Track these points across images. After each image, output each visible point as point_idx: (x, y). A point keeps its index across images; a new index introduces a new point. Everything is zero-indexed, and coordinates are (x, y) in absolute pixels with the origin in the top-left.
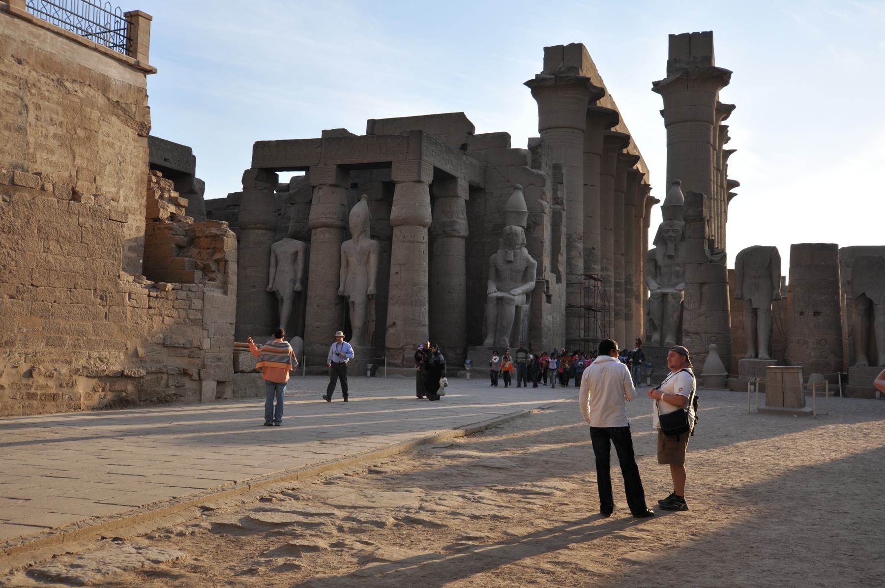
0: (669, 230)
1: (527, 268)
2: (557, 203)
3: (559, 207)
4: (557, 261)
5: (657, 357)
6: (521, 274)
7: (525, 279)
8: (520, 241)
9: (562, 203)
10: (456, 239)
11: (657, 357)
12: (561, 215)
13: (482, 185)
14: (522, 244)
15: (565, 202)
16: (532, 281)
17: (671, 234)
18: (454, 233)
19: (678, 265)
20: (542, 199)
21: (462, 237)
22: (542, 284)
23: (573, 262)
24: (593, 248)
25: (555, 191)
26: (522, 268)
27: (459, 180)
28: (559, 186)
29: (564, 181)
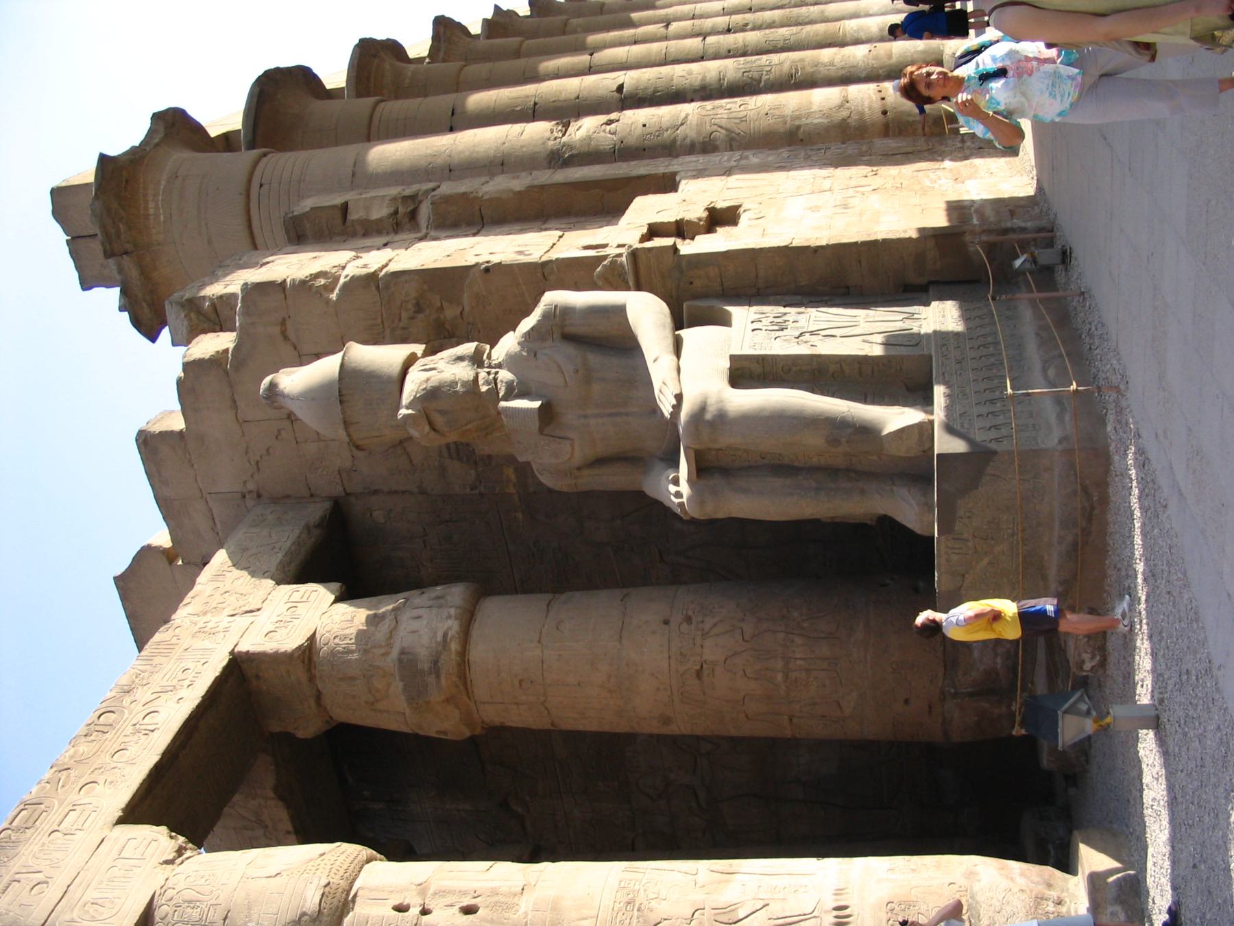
2: (413, 215)
3: (425, 211)
7: (618, 342)
8: (464, 372)
10: (479, 652)
12: (447, 199)
13: (316, 511)
14: (477, 360)
15: (409, 191)
16: (620, 310)
18: (449, 661)
20: (329, 288)
21: (468, 618)
22: (638, 271)
26: (565, 355)
27: (248, 645)
28: (353, 216)
29: (338, 200)
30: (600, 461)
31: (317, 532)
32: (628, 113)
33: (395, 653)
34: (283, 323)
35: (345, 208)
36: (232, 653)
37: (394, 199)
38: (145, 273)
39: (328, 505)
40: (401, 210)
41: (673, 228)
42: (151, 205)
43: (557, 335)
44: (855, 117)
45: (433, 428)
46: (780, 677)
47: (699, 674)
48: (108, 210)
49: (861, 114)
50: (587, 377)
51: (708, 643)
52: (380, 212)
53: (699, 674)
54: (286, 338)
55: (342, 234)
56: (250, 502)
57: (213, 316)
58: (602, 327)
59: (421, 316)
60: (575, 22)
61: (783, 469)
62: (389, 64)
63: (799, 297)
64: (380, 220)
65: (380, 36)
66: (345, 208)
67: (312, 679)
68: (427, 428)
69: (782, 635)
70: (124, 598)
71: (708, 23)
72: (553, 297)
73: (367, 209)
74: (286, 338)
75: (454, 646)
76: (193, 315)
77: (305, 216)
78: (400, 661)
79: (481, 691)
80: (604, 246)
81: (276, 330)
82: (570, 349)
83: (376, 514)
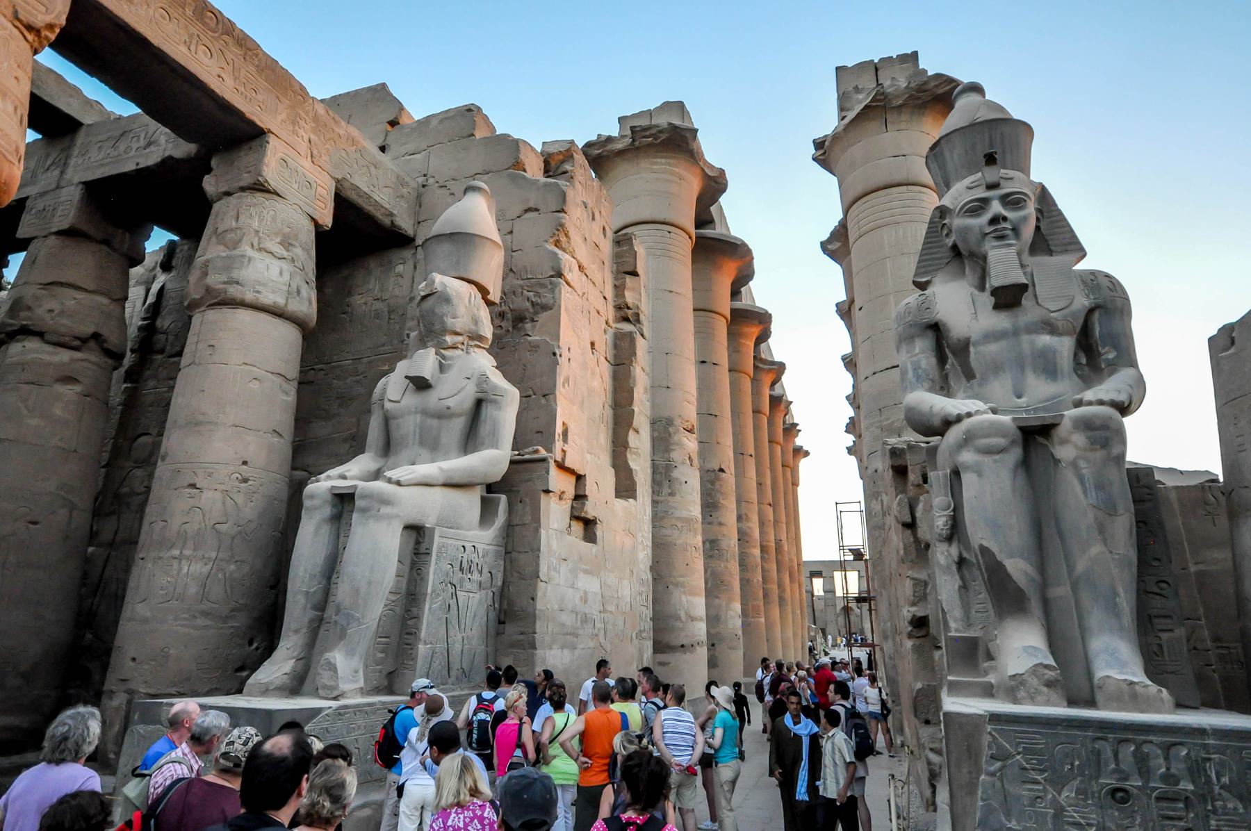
0: (985, 202)
1: (479, 403)
3: (627, 327)
4: (626, 446)
5: (1119, 796)
6: (458, 426)
9: (638, 321)
10: (243, 315)
11: (1119, 796)
16: (495, 445)
17: (996, 207)
18: (233, 291)
19: (1050, 328)
20: (557, 243)
23: (675, 474)
24: (722, 470)
25: (619, 289)
28: (629, 279)
29: (640, 270)
30: (387, 420)
31: (387, 221)
32: (698, 474)
33: (250, 252)
34: (536, 210)
35: (634, 274)
36: (270, 131)
37: (638, 308)
38: (621, 153)
39: (410, 232)
40: (630, 312)
41: (581, 493)
42: (663, 161)
43: (480, 395)
44: (678, 624)
45: (424, 298)
46: (176, 552)
47: (193, 486)
48: (661, 132)
49: (682, 629)
50: (444, 415)
51: (218, 495)
52: (630, 297)
53: (193, 486)
54: (526, 211)
55: (618, 272)
56: (421, 180)
57: (560, 170)
58: (484, 429)
59: (528, 305)
60: (779, 449)
61: (332, 566)
62: (754, 331)
63: (500, 583)
64: (624, 296)
65: (773, 327)
66: (634, 274)
67: (243, 189)
68: (423, 294)
69: (213, 555)
70: (370, 89)
71: (771, 532)
72: (511, 396)
73: (633, 289)
74: (526, 211)
75: (249, 297)
76: (561, 157)
77: (631, 245)
78: (243, 256)
79: (212, 315)
80: (565, 440)
81: (532, 205)
82: (468, 404)
83: (401, 267)
